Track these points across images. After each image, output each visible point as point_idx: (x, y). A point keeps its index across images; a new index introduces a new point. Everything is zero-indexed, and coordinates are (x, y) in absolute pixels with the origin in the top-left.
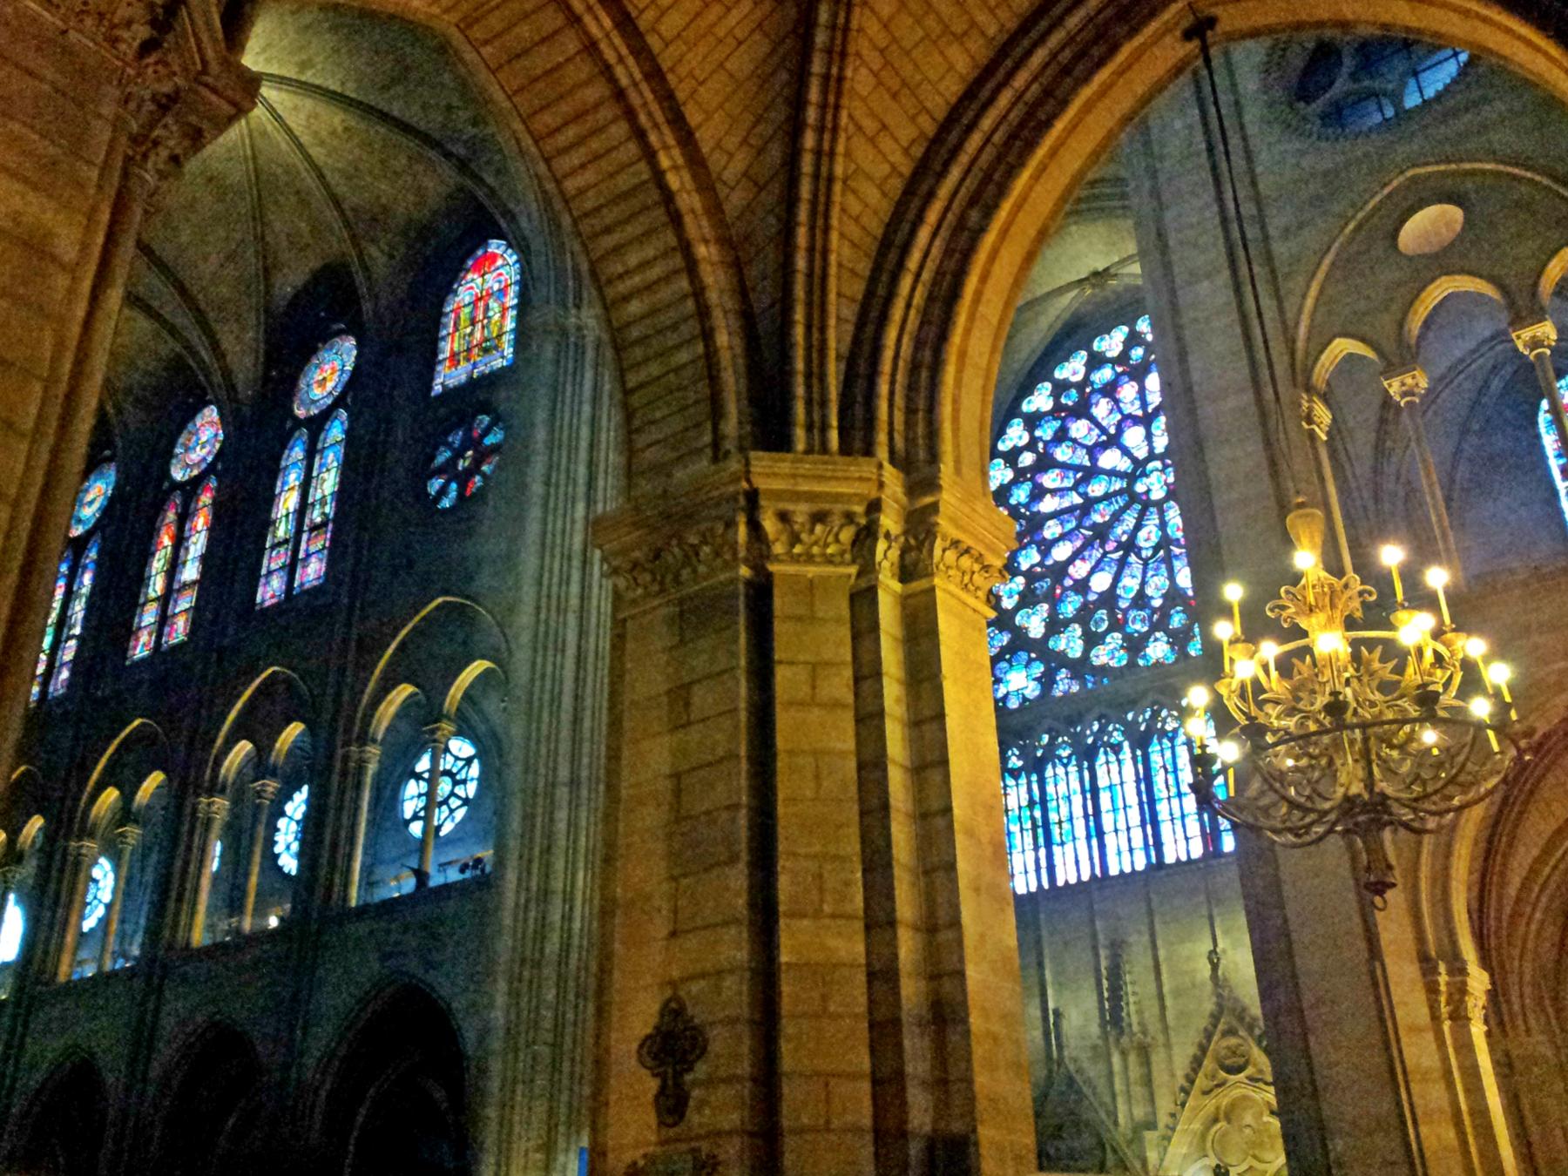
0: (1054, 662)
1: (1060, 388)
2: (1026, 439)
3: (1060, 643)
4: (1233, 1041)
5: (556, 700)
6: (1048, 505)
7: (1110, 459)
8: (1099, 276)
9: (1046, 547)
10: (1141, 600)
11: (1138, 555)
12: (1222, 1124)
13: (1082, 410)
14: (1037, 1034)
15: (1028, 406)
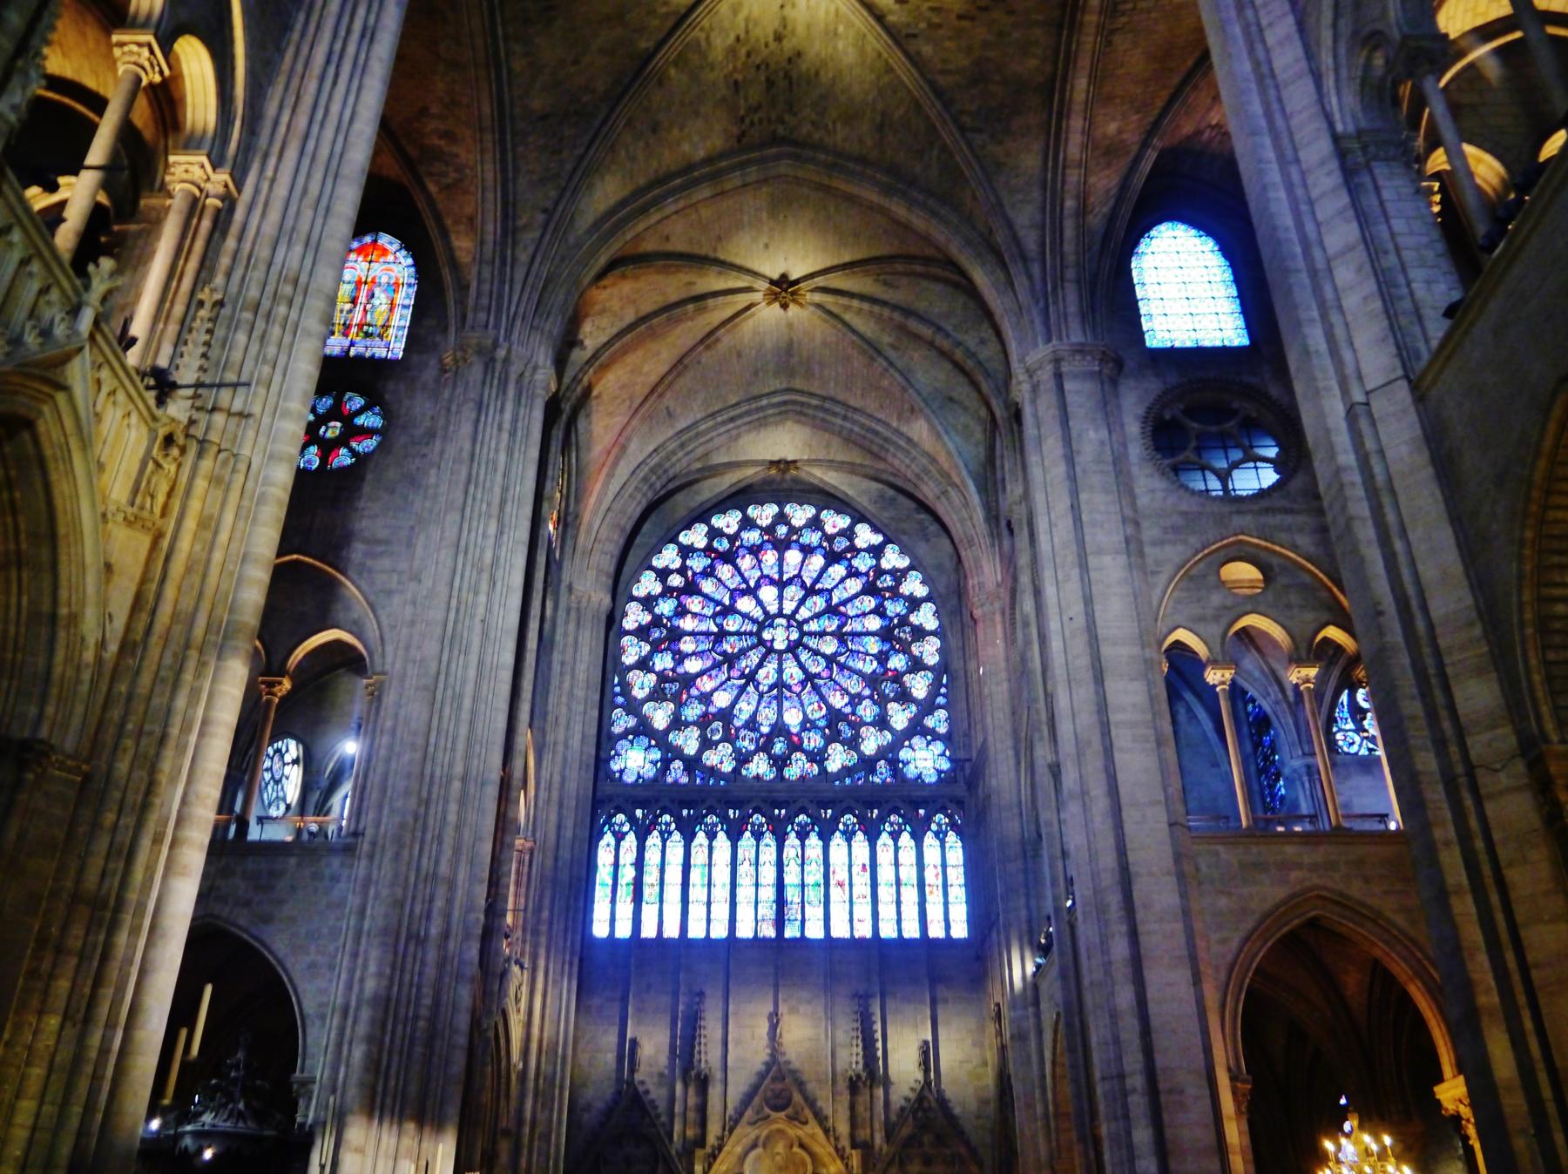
0: (671, 753)
1: (714, 533)
2: (677, 564)
3: (676, 738)
4: (779, 1086)
5: (458, 698)
6: (687, 624)
7: (745, 604)
8: (783, 465)
9: (680, 658)
10: (752, 724)
11: (756, 688)
12: (759, 1150)
13: (729, 558)
14: (611, 1057)
15: (684, 538)
